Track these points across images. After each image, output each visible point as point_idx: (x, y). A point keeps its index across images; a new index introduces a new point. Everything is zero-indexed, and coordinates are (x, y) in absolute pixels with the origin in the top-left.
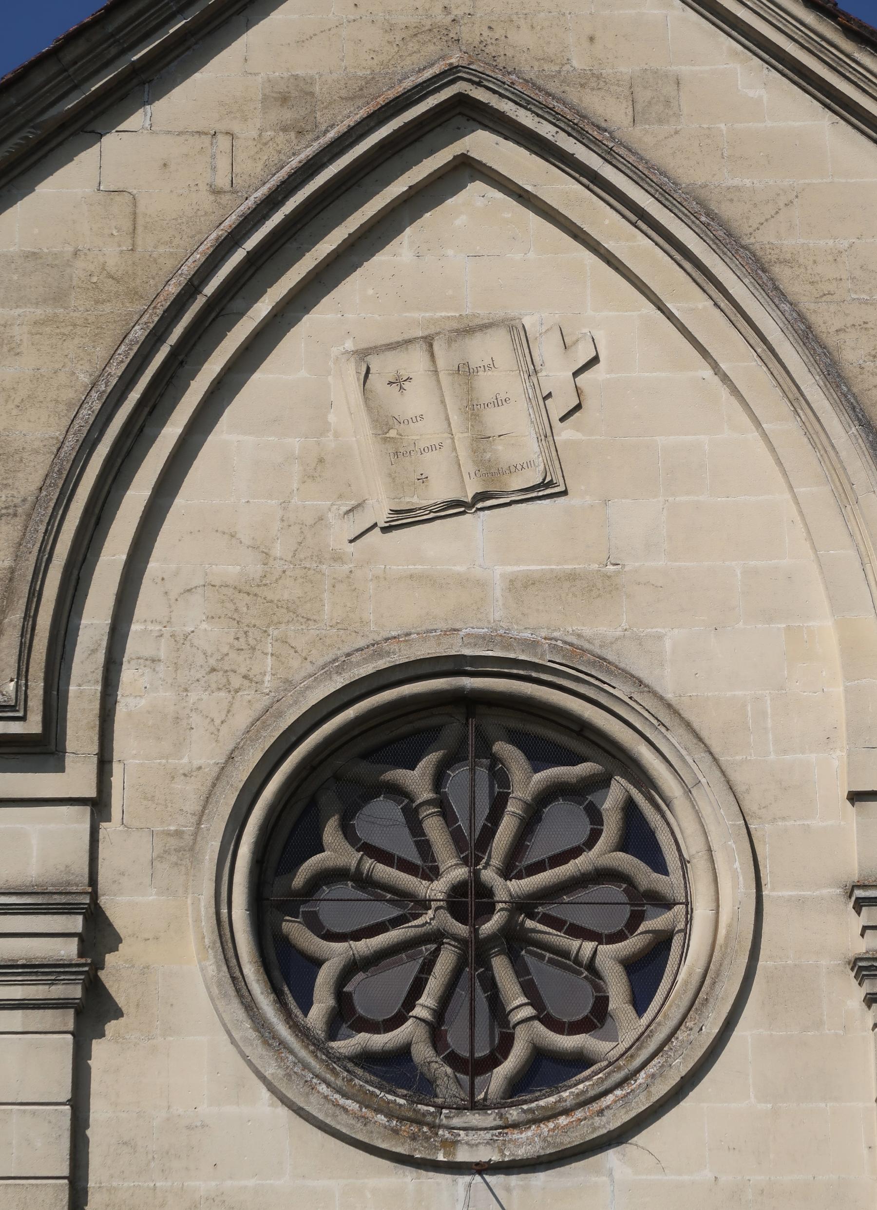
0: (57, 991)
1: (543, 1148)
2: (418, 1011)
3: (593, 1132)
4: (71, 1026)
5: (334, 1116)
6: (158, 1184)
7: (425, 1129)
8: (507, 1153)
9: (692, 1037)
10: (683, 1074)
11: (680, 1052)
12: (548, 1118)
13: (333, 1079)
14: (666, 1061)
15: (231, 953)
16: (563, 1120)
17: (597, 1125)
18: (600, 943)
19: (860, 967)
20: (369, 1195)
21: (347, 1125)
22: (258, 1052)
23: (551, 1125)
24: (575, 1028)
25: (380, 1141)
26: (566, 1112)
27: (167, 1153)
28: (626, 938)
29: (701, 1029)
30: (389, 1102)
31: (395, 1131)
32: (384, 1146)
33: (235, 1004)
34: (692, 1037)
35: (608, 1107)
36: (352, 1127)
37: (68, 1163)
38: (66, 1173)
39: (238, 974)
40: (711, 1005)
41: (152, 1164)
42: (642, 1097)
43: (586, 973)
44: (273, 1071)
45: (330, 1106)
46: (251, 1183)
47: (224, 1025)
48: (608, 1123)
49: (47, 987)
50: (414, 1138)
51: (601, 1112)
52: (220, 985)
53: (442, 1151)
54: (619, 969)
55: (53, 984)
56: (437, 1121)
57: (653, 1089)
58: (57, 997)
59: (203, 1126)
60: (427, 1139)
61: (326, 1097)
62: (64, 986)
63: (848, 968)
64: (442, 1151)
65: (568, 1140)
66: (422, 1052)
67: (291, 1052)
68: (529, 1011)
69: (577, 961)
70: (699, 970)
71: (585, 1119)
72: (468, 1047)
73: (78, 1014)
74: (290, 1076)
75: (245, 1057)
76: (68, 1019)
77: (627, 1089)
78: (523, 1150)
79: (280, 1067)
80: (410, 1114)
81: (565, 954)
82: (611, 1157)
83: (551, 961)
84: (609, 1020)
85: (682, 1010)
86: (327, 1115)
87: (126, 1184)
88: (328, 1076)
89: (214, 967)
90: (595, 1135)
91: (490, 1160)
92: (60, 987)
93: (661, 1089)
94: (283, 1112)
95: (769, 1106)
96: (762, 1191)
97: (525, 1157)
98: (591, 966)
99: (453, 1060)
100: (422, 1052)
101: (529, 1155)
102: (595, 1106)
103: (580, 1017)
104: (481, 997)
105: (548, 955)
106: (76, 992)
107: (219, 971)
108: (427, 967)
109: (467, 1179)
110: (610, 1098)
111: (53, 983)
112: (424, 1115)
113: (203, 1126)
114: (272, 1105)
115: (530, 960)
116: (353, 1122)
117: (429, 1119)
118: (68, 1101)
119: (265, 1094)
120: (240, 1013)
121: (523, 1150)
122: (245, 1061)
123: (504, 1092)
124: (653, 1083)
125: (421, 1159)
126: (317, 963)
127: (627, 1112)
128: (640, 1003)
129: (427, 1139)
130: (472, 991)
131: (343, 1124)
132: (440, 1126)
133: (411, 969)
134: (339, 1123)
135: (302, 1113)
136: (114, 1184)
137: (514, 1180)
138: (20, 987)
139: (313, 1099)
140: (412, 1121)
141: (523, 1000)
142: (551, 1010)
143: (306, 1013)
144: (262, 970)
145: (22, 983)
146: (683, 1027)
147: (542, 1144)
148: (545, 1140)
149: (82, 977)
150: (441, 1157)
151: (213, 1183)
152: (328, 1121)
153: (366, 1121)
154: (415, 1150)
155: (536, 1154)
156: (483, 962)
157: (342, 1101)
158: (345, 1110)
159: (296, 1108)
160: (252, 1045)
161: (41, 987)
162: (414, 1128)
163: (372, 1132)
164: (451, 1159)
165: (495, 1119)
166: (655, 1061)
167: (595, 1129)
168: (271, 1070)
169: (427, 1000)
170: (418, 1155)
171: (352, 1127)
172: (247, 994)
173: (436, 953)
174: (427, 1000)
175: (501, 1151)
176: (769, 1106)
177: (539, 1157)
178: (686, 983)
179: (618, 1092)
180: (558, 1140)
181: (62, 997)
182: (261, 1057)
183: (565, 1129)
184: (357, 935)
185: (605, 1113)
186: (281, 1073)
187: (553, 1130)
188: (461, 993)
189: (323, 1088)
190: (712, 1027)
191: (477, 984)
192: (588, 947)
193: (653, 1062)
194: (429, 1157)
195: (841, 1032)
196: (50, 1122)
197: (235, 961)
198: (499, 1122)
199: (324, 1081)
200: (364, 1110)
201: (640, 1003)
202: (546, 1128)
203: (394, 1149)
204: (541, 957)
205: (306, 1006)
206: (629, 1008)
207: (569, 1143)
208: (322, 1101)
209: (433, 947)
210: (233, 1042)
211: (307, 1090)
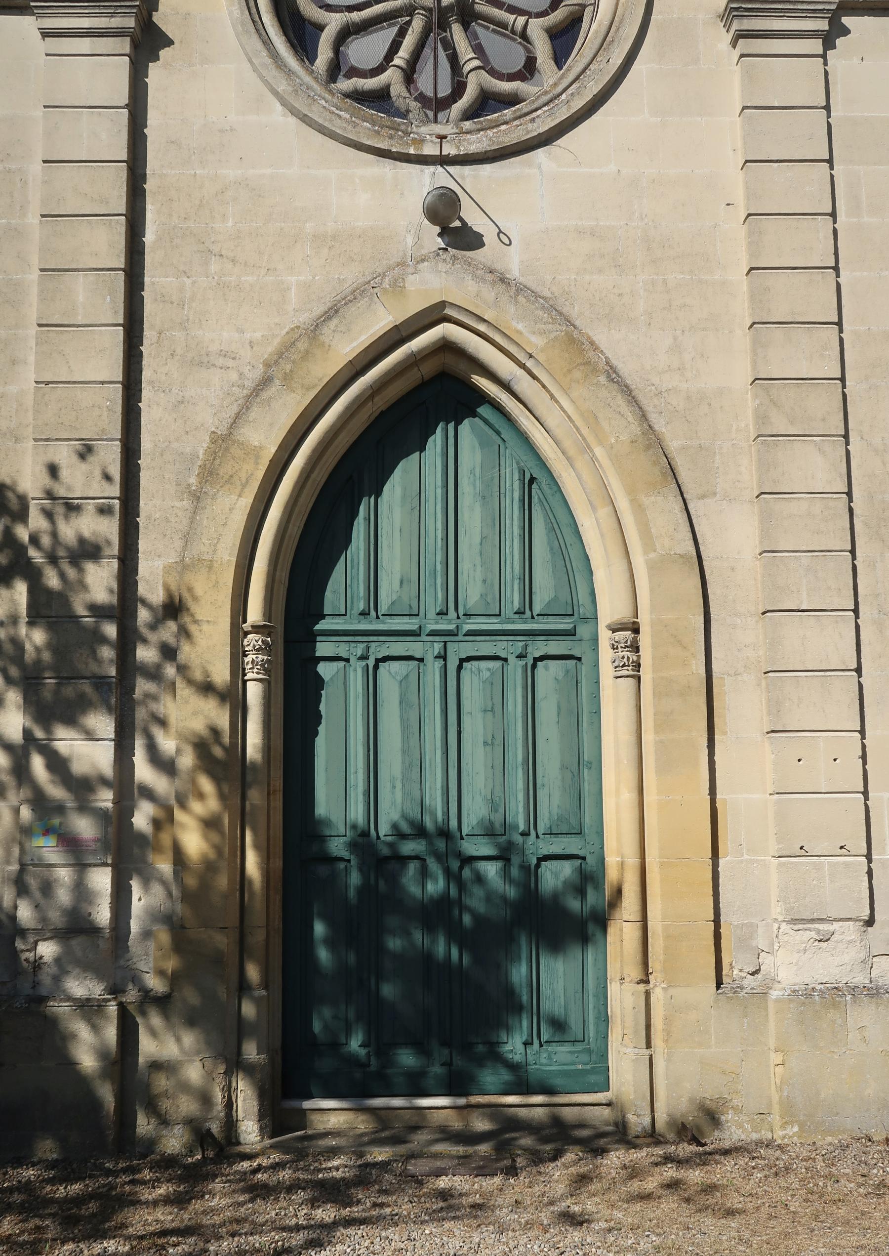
0: (116, 22)
1: (489, 146)
2: (397, 61)
3: (526, 134)
4: (127, 50)
5: (331, 121)
6: (197, 172)
7: (400, 133)
8: (462, 149)
9: (602, 66)
10: (595, 93)
11: (592, 77)
12: (493, 128)
13: (330, 98)
14: (582, 84)
15: (254, 10)
16: (503, 127)
17: (530, 129)
18: (530, 17)
19: (731, 8)
20: (357, 181)
21: (341, 128)
22: (272, 74)
23: (495, 130)
24: (511, 78)
25: (365, 139)
26: (506, 123)
27: (204, 149)
28: (549, 14)
29: (608, 61)
30: (372, 115)
31: (378, 132)
32: (369, 143)
33: (255, 37)
34: (602, 66)
35: (538, 117)
36: (344, 129)
37: (126, 150)
38: (125, 157)
39: (257, 19)
40: (616, 43)
41: (193, 157)
42: (564, 109)
43: (520, 40)
44: (284, 88)
45: (328, 113)
46: (269, 171)
47: (246, 54)
48: (539, 127)
49: (108, 19)
50: (391, 137)
51: (533, 120)
52: (243, 24)
53: (413, 147)
54: (544, 35)
55: (112, 17)
56: (409, 129)
57: (572, 104)
58: (115, 26)
59: (231, 130)
60: (402, 138)
61: (324, 107)
62: (121, 19)
63: (719, 20)
64: (413, 147)
65: (508, 139)
66: (398, 90)
67: (299, 77)
68: (476, 63)
69: (513, 32)
70: (606, 23)
71: (521, 125)
72: (433, 90)
73: (135, 45)
74: (297, 91)
75: (261, 77)
76: (124, 44)
77: (552, 105)
78: (474, 147)
79: (289, 85)
80: (388, 124)
81: (503, 25)
82: (540, 155)
83: (494, 31)
84: (537, 75)
85: (594, 51)
86: (325, 120)
87: (173, 172)
88: (327, 96)
89: (238, 11)
90: (528, 137)
91: (449, 154)
92: (118, 19)
93: (578, 104)
94: (292, 121)
95: (659, 119)
96: (654, 180)
97: (476, 151)
98: (524, 36)
99: (422, 99)
100: (398, 90)
101: (478, 151)
102: (528, 118)
103: (516, 70)
104: (442, 54)
105: (492, 26)
106: (130, 22)
107: (242, 14)
108: (402, 33)
109: (432, 168)
110: (539, 112)
111: (112, 15)
112: (399, 124)
113: (231, 130)
114: (284, 115)
115: (479, 30)
116: (345, 125)
117: (403, 127)
118: (126, 105)
119: (278, 107)
120: (259, 45)
121: (474, 147)
122: (262, 81)
123: (460, 117)
124: (573, 100)
125: (397, 152)
126: (321, 28)
127: (552, 120)
128: (560, 58)
129: (402, 138)
130: (436, 48)
131: (338, 127)
132: (411, 133)
133: (391, 33)
134: (334, 126)
135: (306, 119)
136: (165, 172)
137: (467, 170)
138: (87, 19)
139: (314, 108)
140: (390, 128)
141: (472, 55)
142: (496, 64)
143: (313, 65)
144: (276, 19)
145: (88, 15)
146: (594, 62)
147: (488, 142)
148: (490, 139)
149: (135, 11)
150: (412, 151)
151: (240, 172)
152: (326, 124)
153: (355, 125)
154: (392, 146)
155: (484, 150)
156: (444, 25)
157: (337, 112)
158: (340, 117)
159: (301, 116)
160: (267, 68)
161: (103, 19)
162: (392, 132)
163: (359, 133)
164: (419, 152)
165: (453, 128)
166: (574, 86)
167: (528, 132)
168: (283, 86)
169: (404, 53)
170: (394, 150)
171: (344, 129)
172: (265, 34)
173: (409, 23)
174: (404, 53)
175: (458, 147)
176: (659, 119)
177: (486, 152)
178: (596, 32)
179: (546, 108)
180: (500, 140)
181: (120, 26)
182: (275, 77)
183: (506, 132)
184: (351, 9)
185: (536, 120)
186: (290, 89)
187: (497, 133)
188: (427, 51)
189: (323, 102)
190: (617, 58)
191: (439, 45)
192: (521, 20)
193: (572, 87)
194: (403, 151)
195: (714, 67)
196: (112, 120)
197: (255, 10)
198: (457, 131)
199: (324, 99)
200: (353, 118)
201: (560, 58)
202: (490, 133)
203: (376, 146)
204: (487, 28)
205: (312, 59)
206: (553, 63)
207: (509, 142)
208: (322, 110)
209: (408, 18)
210: (255, 70)
211: (310, 101)
